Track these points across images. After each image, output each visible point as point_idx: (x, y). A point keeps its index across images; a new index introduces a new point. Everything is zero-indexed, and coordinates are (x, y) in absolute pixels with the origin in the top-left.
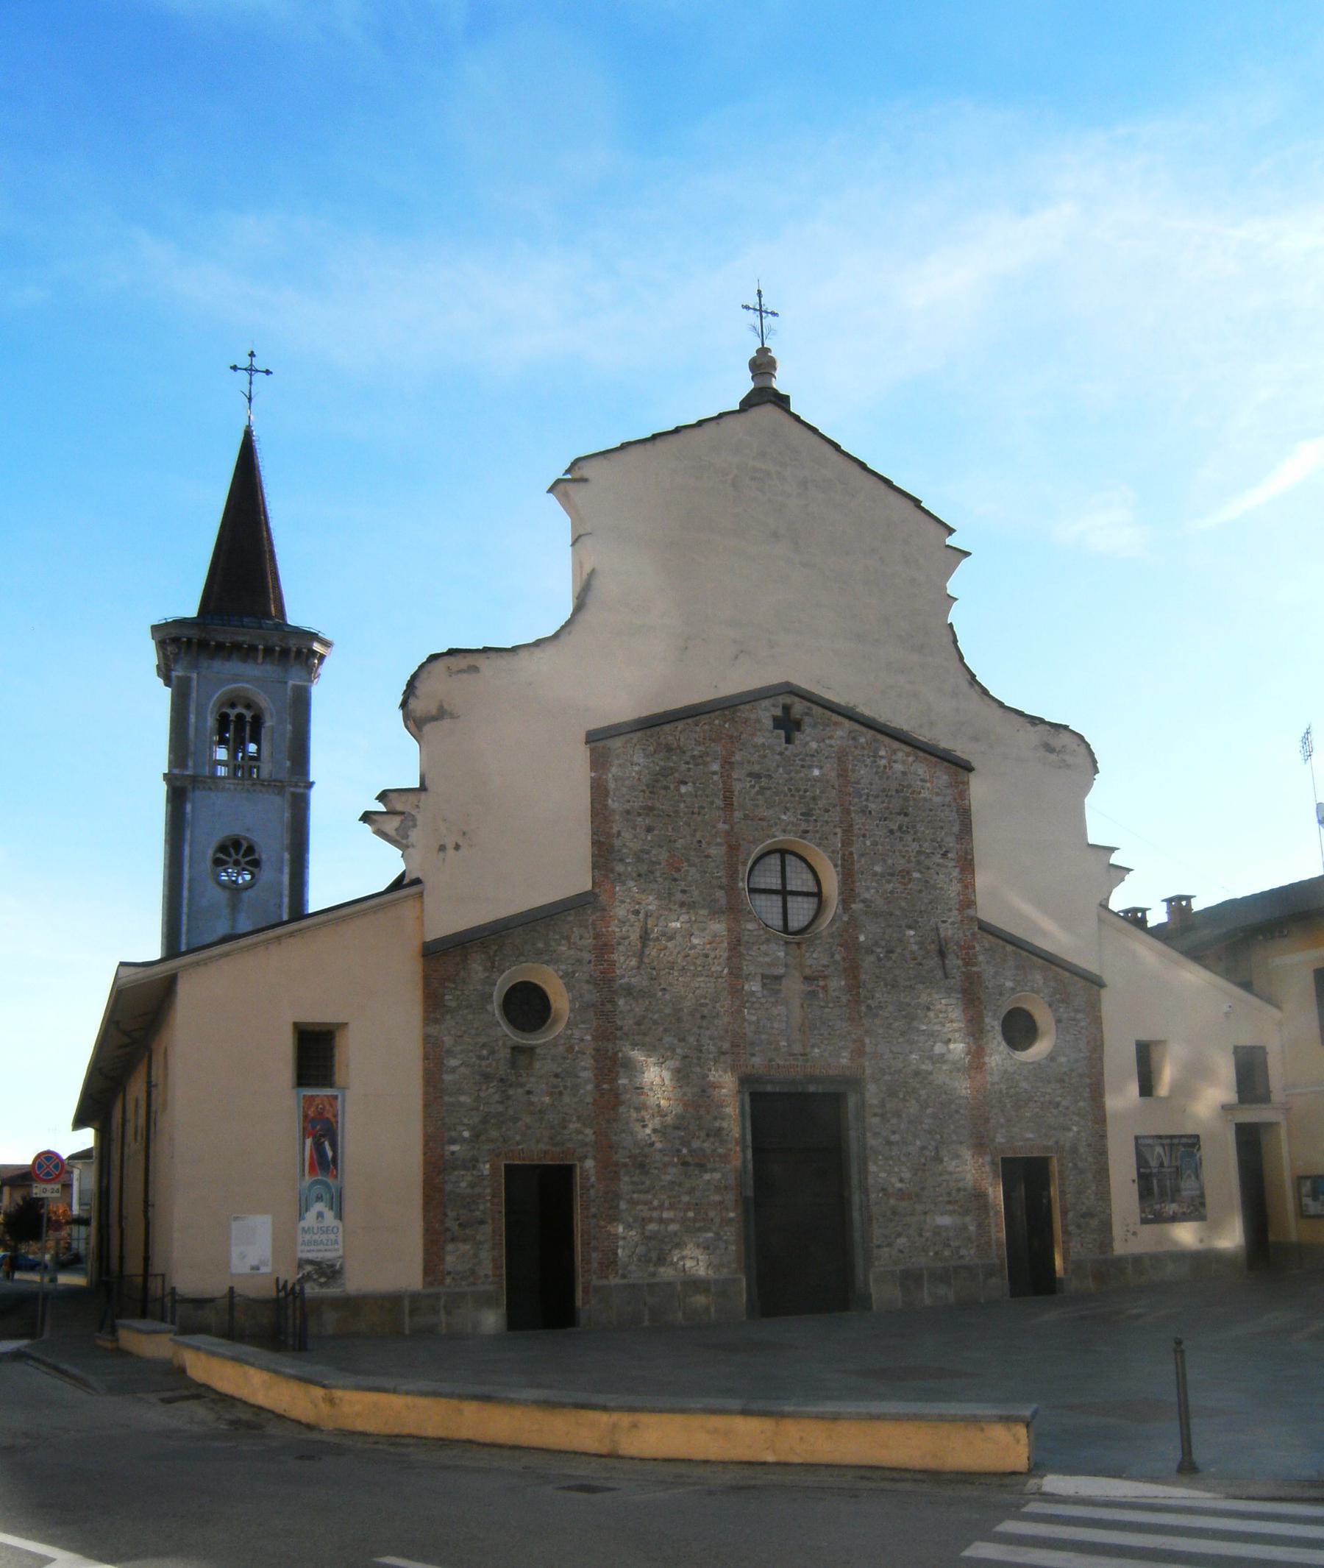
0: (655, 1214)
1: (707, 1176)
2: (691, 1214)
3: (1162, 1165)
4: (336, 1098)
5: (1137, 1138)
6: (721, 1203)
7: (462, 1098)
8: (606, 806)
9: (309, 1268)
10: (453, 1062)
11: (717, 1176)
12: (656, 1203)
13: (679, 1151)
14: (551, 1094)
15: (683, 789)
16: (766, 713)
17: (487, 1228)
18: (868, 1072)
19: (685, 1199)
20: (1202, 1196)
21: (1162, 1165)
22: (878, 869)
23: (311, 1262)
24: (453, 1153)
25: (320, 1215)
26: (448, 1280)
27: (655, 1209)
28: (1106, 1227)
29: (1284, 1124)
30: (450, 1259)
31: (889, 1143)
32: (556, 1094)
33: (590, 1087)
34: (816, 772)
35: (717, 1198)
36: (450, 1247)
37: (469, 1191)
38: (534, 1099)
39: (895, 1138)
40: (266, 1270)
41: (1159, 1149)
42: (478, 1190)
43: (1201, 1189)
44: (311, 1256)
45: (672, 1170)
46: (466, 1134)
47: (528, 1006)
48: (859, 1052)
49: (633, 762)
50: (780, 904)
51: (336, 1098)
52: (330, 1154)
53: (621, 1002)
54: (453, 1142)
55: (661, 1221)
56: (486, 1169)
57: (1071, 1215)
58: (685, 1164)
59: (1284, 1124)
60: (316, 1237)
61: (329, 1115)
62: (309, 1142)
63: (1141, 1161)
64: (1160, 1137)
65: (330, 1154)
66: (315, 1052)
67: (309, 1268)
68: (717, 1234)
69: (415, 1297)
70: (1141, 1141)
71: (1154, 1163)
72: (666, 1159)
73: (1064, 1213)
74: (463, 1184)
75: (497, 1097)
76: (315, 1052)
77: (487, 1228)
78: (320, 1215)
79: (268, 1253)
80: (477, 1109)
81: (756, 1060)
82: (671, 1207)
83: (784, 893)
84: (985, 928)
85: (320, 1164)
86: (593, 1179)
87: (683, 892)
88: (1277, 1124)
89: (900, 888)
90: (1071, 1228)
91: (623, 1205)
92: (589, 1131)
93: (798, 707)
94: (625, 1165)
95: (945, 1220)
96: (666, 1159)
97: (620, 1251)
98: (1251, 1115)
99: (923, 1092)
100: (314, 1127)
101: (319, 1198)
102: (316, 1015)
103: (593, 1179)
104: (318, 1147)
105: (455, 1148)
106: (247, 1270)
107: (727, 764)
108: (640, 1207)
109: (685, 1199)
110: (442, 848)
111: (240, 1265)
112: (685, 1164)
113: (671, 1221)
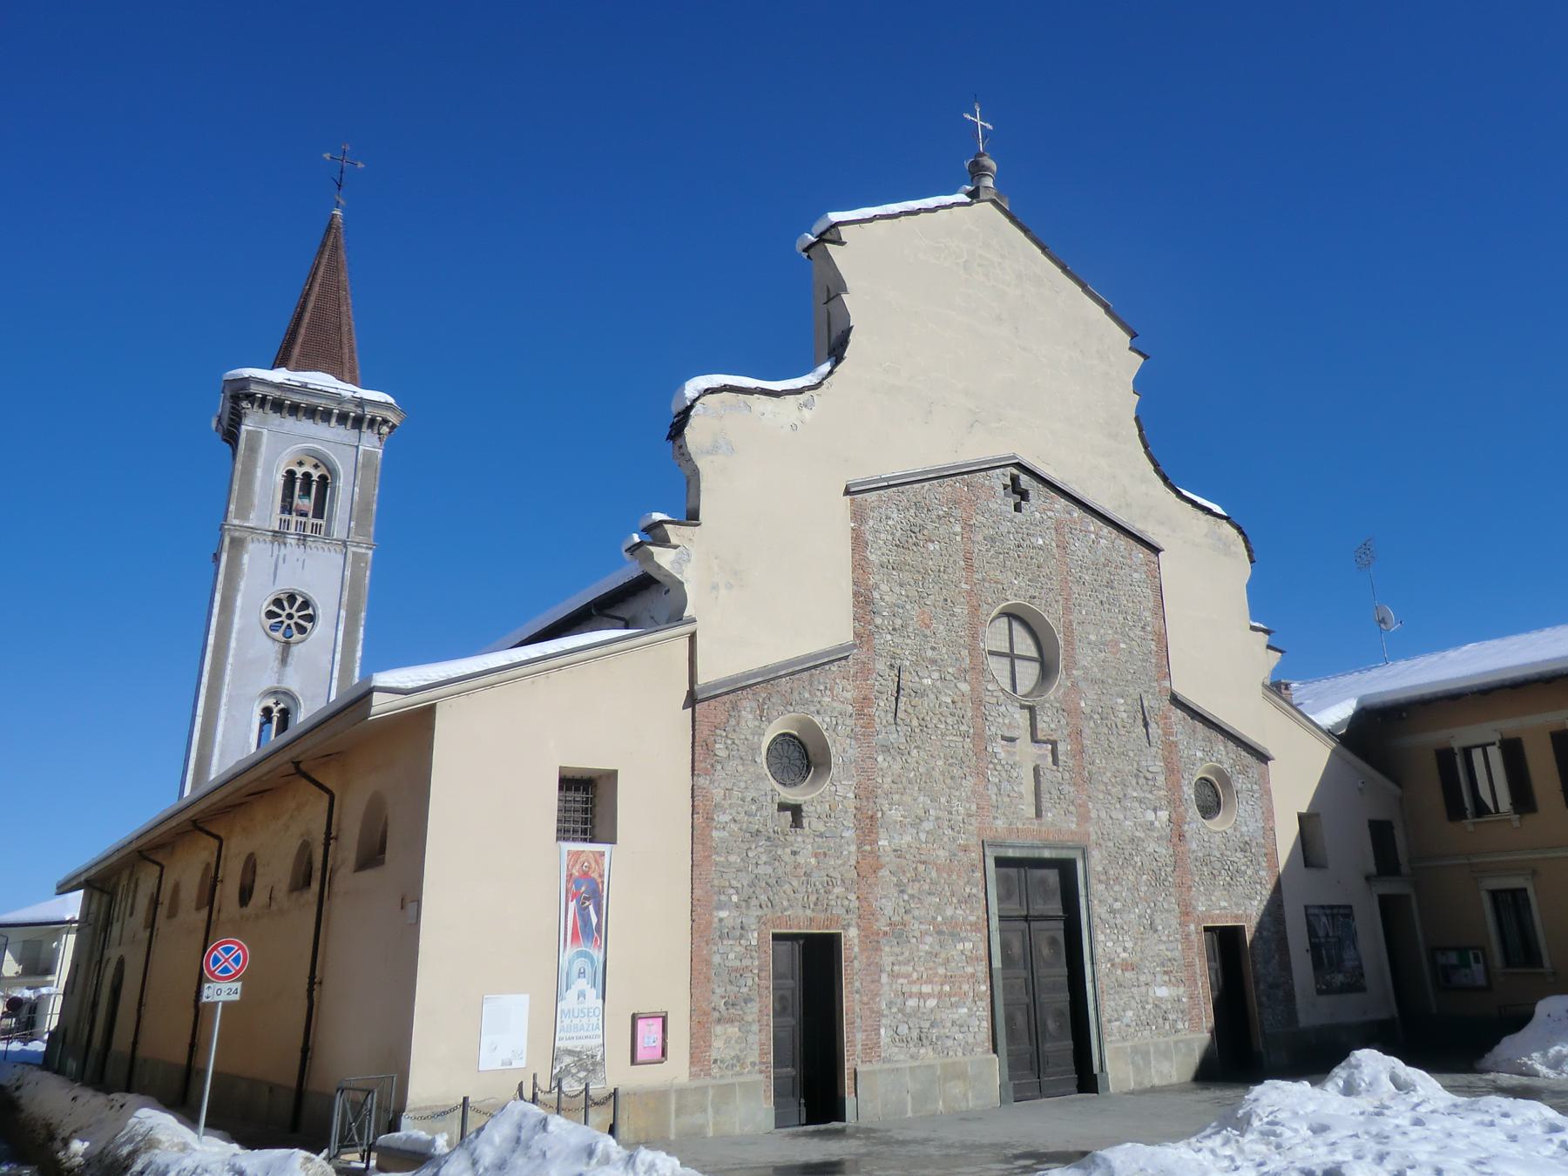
0: (915, 989)
1: (960, 946)
2: (947, 988)
3: (1327, 935)
4: (602, 854)
5: (1306, 907)
6: (973, 975)
7: (732, 858)
8: (865, 558)
9: (568, 1060)
10: (725, 818)
11: (969, 945)
12: (915, 976)
13: (934, 919)
14: (816, 856)
15: (931, 547)
16: (1001, 478)
17: (753, 1010)
18: (1093, 837)
19: (941, 971)
20: (1360, 967)
21: (1327, 935)
22: (1093, 638)
23: (570, 1052)
24: (721, 920)
25: (582, 994)
26: (715, 1070)
27: (914, 982)
28: (1290, 997)
29: (1414, 898)
30: (718, 1044)
31: (1112, 911)
32: (820, 855)
33: (853, 848)
34: (1040, 542)
35: (970, 970)
36: (719, 1029)
37: (738, 963)
38: (801, 859)
39: (1118, 905)
40: (519, 1063)
41: (1324, 919)
42: (746, 962)
43: (1359, 959)
44: (570, 1045)
45: (929, 939)
46: (735, 898)
47: (801, 756)
48: (1084, 818)
49: (890, 516)
50: (1008, 667)
51: (602, 854)
52: (594, 919)
53: (880, 759)
54: (721, 907)
55: (920, 995)
56: (753, 938)
57: (1262, 987)
58: (940, 933)
59: (1414, 898)
60: (576, 1021)
61: (595, 875)
62: (572, 905)
63: (1312, 931)
64: (1323, 907)
65: (594, 919)
66: (586, 801)
67: (568, 1060)
68: (970, 1009)
69: (681, 1092)
70: (1311, 911)
71: (1321, 933)
72: (923, 927)
73: (1257, 983)
74: (732, 956)
75: (764, 858)
76: (586, 801)
77: (753, 1010)
78: (582, 994)
79: (522, 1044)
80: (746, 868)
81: (1000, 824)
82: (930, 981)
83: (1012, 656)
84: (1176, 701)
85: (584, 933)
86: (856, 949)
87: (933, 649)
88: (1525, 890)
89: (1110, 657)
90: (1264, 999)
91: (884, 978)
92: (852, 897)
93: (1025, 480)
94: (885, 934)
95: (1162, 992)
96: (923, 927)
97: (882, 1031)
98: (1390, 887)
99: (1137, 859)
100: (578, 888)
101: (582, 974)
102: (587, 760)
103: (856, 949)
104: (582, 912)
105: (723, 914)
106: (497, 1066)
107: (968, 526)
108: (901, 981)
109: (941, 971)
110: (715, 587)
111: (489, 1061)
112: (940, 933)
113: (929, 995)
